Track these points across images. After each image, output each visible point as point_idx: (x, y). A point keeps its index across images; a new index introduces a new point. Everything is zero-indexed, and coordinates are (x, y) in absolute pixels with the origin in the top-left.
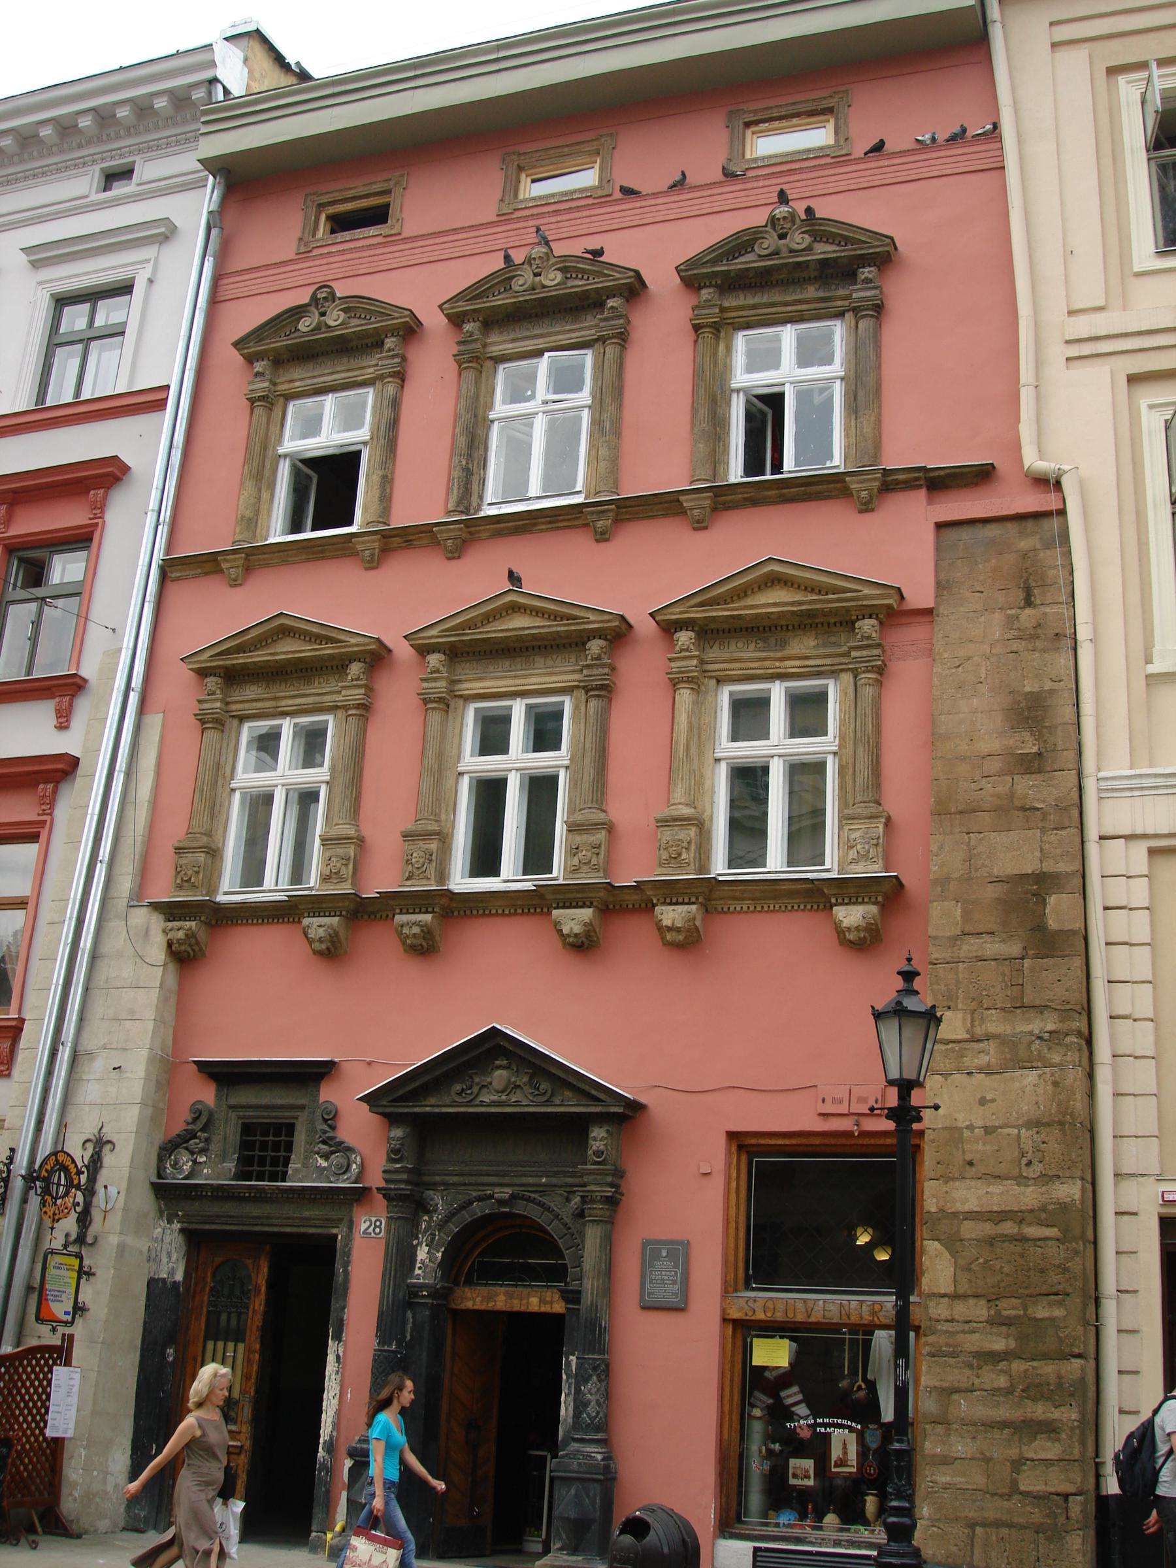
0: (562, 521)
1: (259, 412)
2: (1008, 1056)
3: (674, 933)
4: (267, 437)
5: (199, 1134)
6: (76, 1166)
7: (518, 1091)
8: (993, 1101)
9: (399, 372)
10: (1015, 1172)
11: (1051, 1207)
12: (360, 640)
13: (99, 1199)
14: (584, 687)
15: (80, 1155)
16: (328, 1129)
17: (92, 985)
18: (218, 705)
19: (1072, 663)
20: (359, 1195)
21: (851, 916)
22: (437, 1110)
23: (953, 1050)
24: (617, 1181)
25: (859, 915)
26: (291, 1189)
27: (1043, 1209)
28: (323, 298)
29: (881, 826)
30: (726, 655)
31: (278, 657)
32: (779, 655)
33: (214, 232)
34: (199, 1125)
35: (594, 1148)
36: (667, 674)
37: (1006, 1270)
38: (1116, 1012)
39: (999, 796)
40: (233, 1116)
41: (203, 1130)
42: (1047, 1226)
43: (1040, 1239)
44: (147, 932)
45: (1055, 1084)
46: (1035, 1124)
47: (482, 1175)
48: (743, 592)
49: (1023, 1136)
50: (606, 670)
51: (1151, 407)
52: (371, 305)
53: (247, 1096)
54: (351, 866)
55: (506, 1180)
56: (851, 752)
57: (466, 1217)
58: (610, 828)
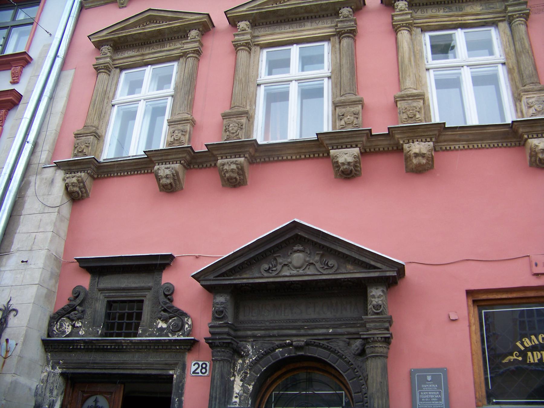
3: (420, 158)
5: (78, 307)
7: (312, 267)
16: (168, 301)
18: (108, 59)
22: (251, 281)
32: (460, 13)
34: (78, 301)
35: (374, 303)
40: (101, 296)
41: (80, 305)
44: (52, 181)
47: (282, 329)
54: (187, 136)
55: (302, 332)
56: (515, 61)
57: (271, 360)
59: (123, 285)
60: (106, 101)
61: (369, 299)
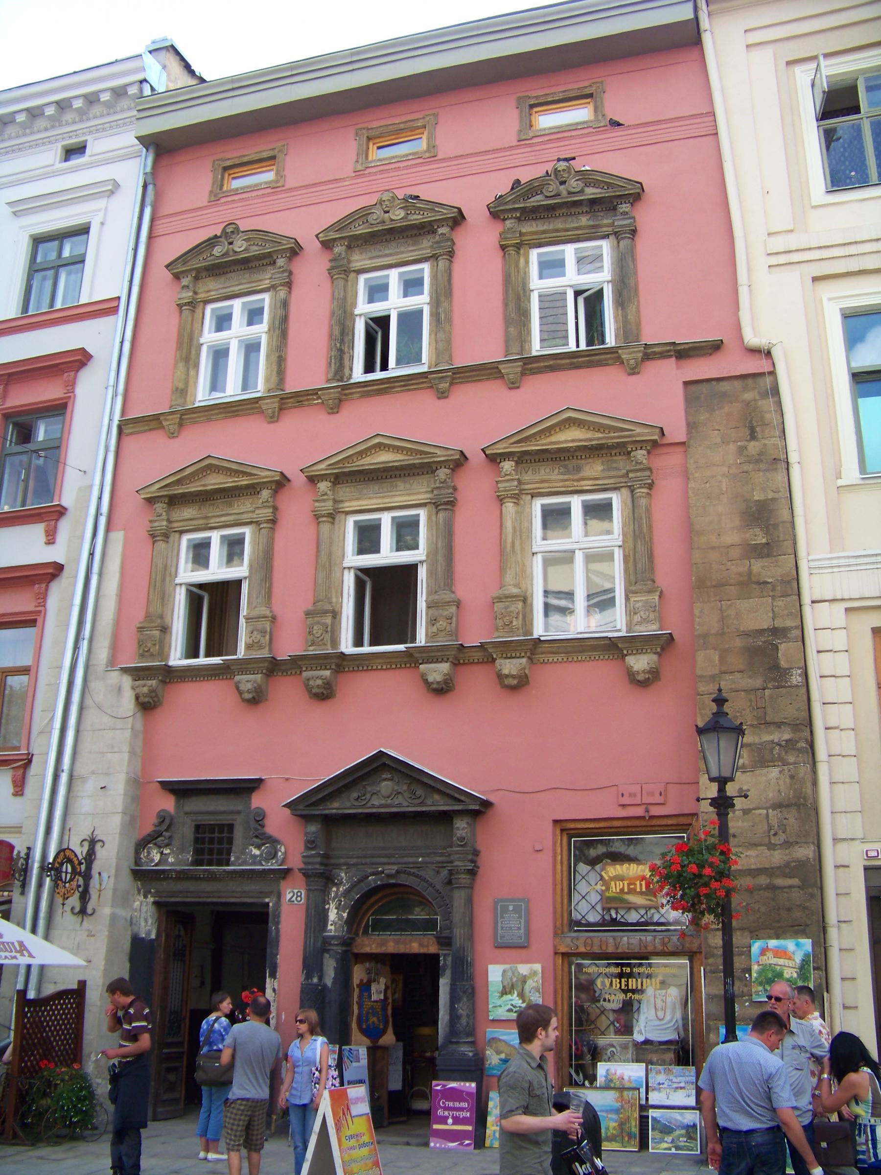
0: (413, 384)
1: (186, 313)
3: (510, 680)
7: (400, 796)
9: (288, 282)
10: (766, 841)
11: (793, 864)
13: (94, 883)
14: (434, 503)
15: (81, 851)
17: (81, 728)
19: (786, 479)
20: (285, 873)
21: (640, 663)
22: (340, 812)
24: (475, 858)
25: (646, 662)
26: (235, 872)
27: (787, 865)
28: (230, 232)
29: (657, 598)
30: (537, 477)
33: (150, 188)
34: (164, 826)
35: (458, 835)
37: (763, 909)
38: (829, 725)
39: (740, 574)
40: (188, 820)
41: (166, 830)
42: (790, 877)
43: (785, 887)
44: (119, 689)
45: (792, 777)
46: (778, 806)
48: (549, 431)
49: (770, 815)
50: (451, 491)
51: (830, 299)
53: (198, 804)
54: (268, 637)
55: (393, 860)
56: (632, 546)
57: (364, 888)
58: (458, 604)
59: (211, 809)
60: (168, 579)
61: (455, 831)
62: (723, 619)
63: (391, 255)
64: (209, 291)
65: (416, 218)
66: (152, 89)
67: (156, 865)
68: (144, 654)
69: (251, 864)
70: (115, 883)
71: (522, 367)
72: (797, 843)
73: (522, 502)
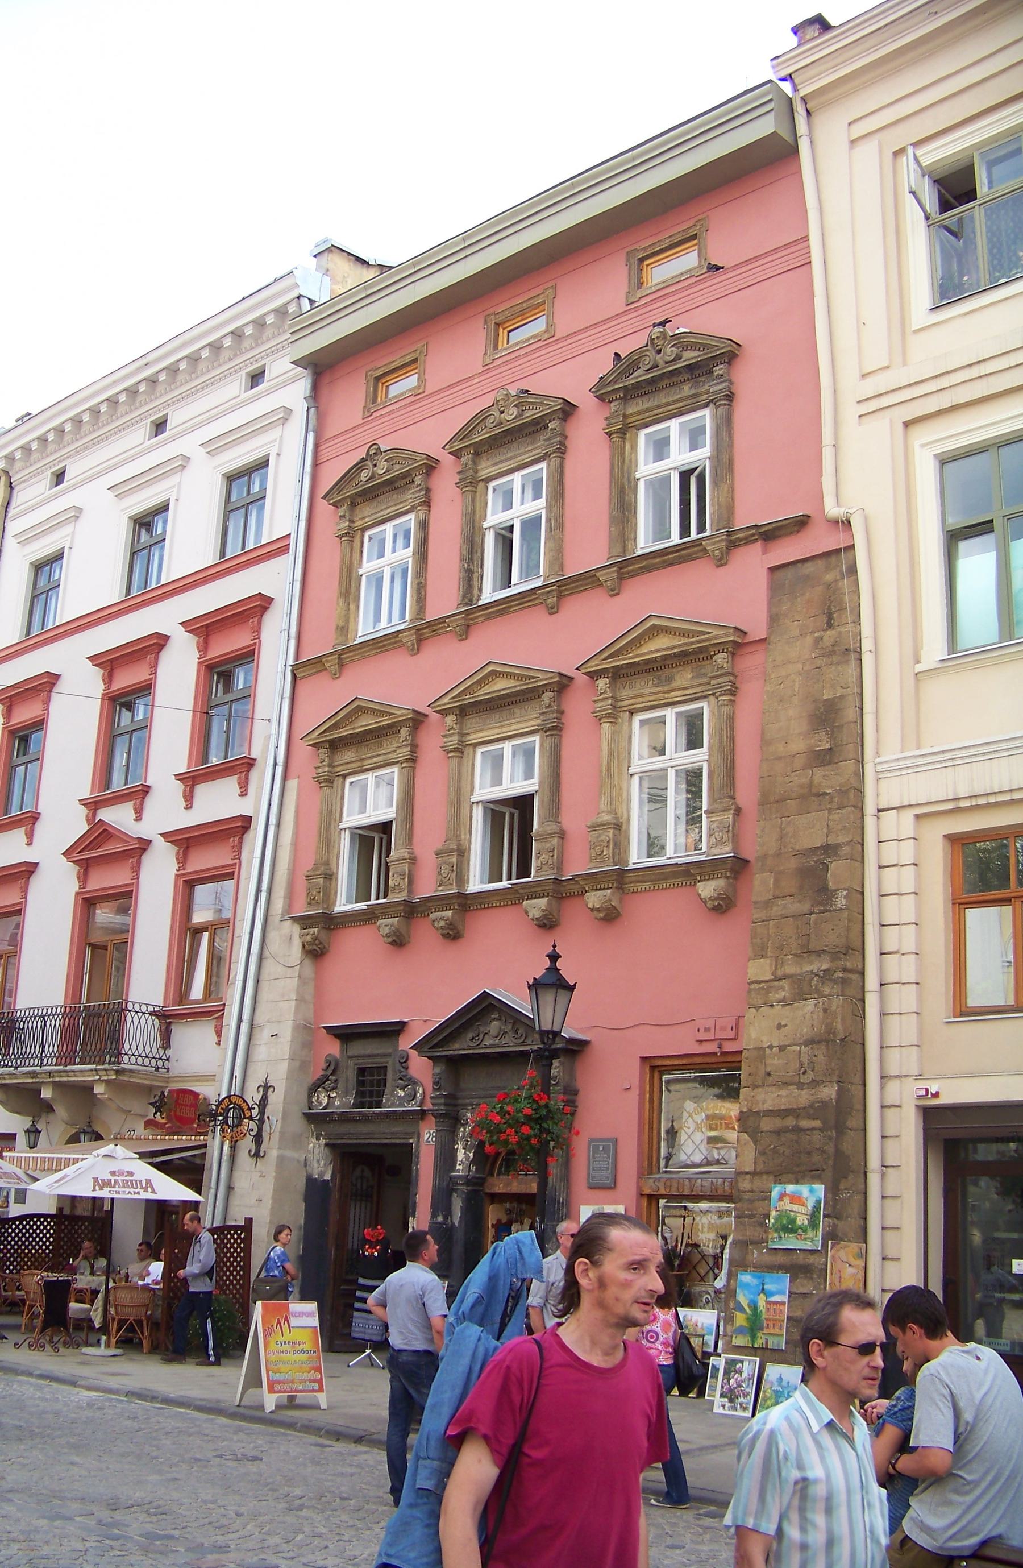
2: (797, 991)
4: (351, 563)
6: (248, 1104)
8: (786, 1026)
9: (424, 501)
10: (796, 1079)
12: (403, 711)
15: (253, 1096)
17: (261, 979)
21: (707, 889)
22: (456, 1053)
23: (763, 988)
27: (811, 1106)
28: (374, 453)
29: (731, 816)
31: (357, 731)
32: (666, 688)
33: (312, 411)
34: (330, 1072)
36: (593, 713)
39: (801, 786)
40: (351, 1063)
42: (814, 1119)
43: (808, 1130)
45: (825, 1011)
46: (810, 1042)
48: (638, 641)
51: (923, 446)
52: (403, 453)
53: (359, 1048)
54: (406, 879)
62: (781, 837)
63: (511, 458)
64: (363, 518)
65: (530, 415)
66: (311, 301)
67: (325, 1108)
68: (311, 902)
69: (398, 1107)
70: (282, 1127)
71: (618, 572)
72: (823, 1082)
73: (620, 720)
